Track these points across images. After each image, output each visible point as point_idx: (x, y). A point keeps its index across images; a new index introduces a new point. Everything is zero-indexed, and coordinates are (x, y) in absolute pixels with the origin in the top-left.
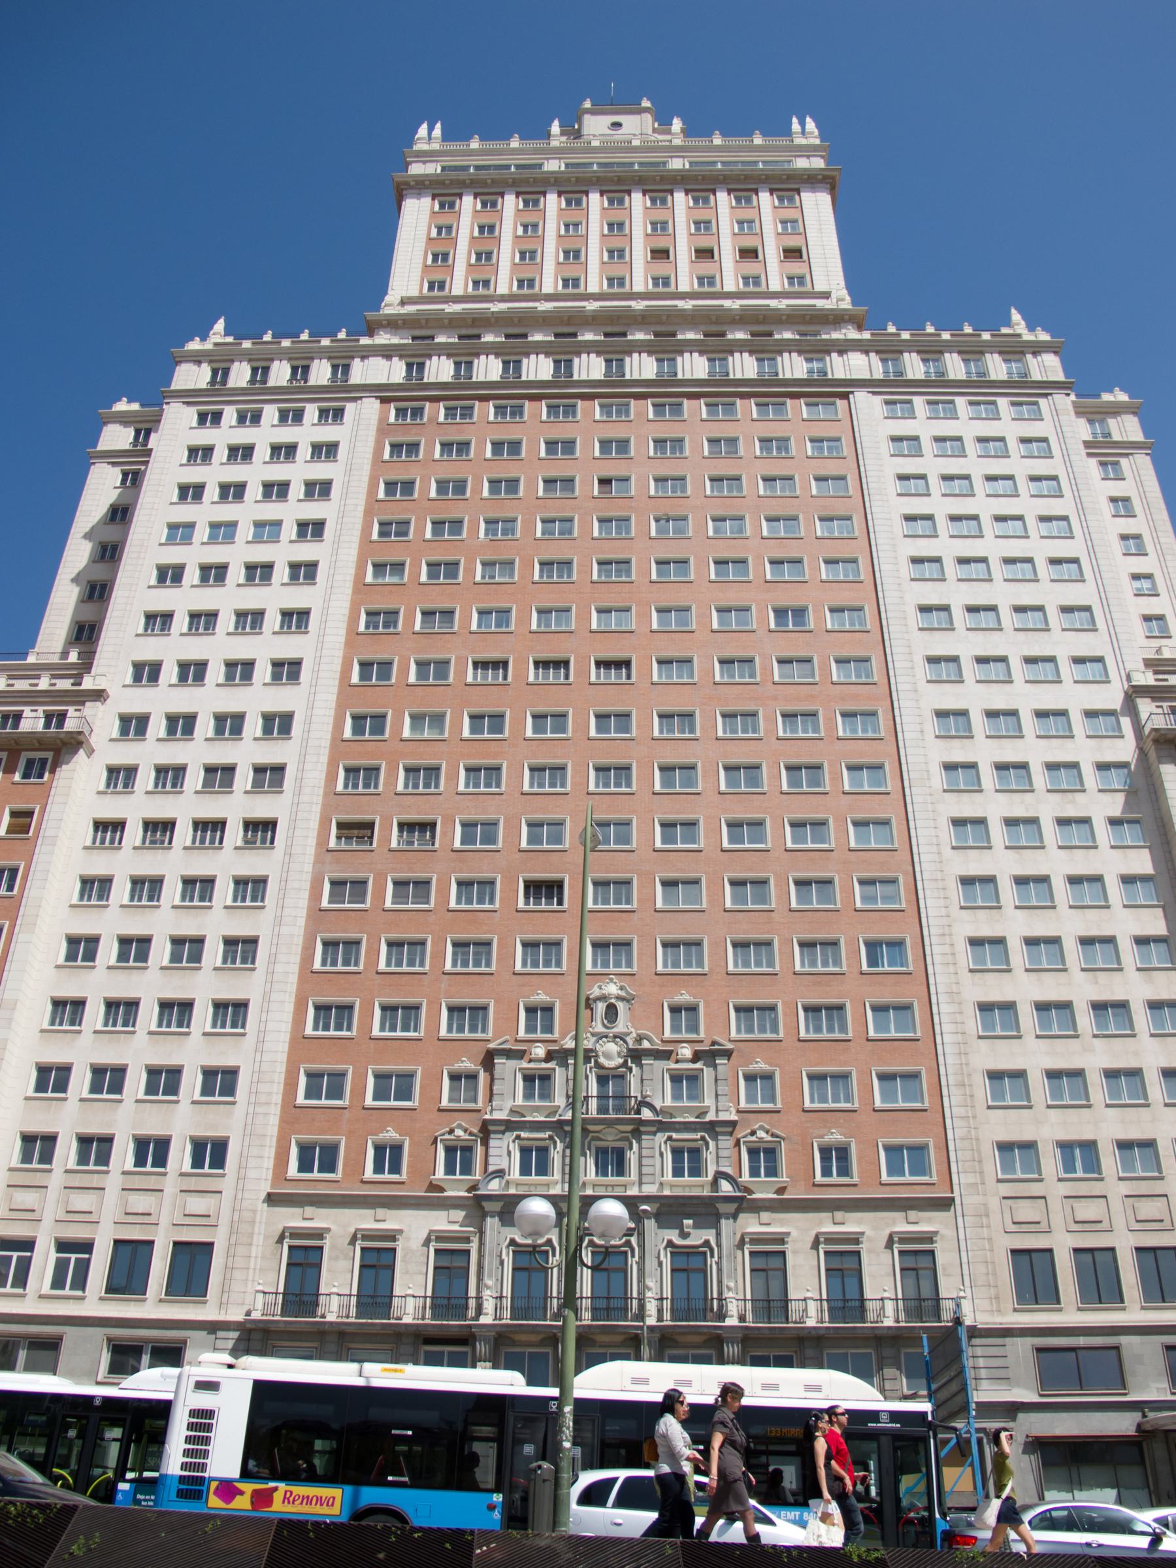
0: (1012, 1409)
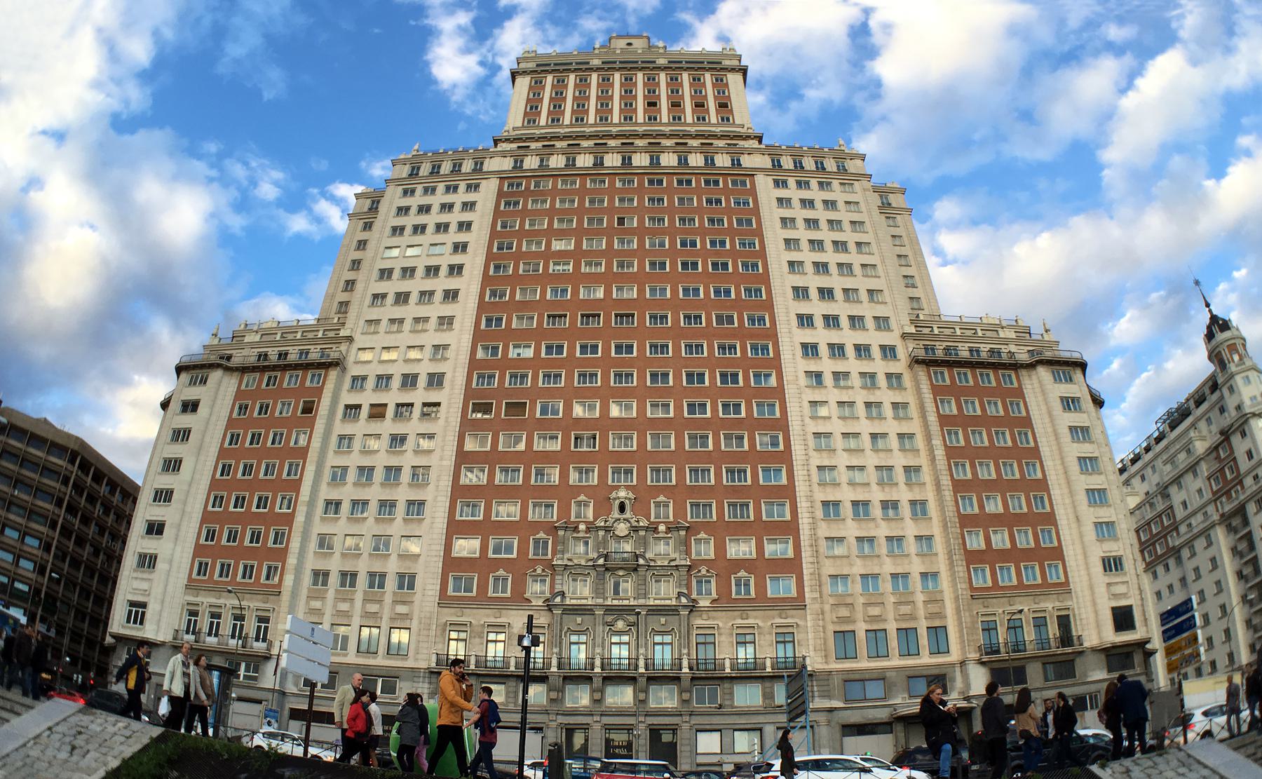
0: (831, 710)
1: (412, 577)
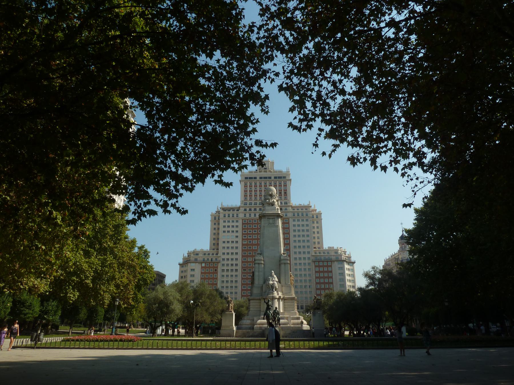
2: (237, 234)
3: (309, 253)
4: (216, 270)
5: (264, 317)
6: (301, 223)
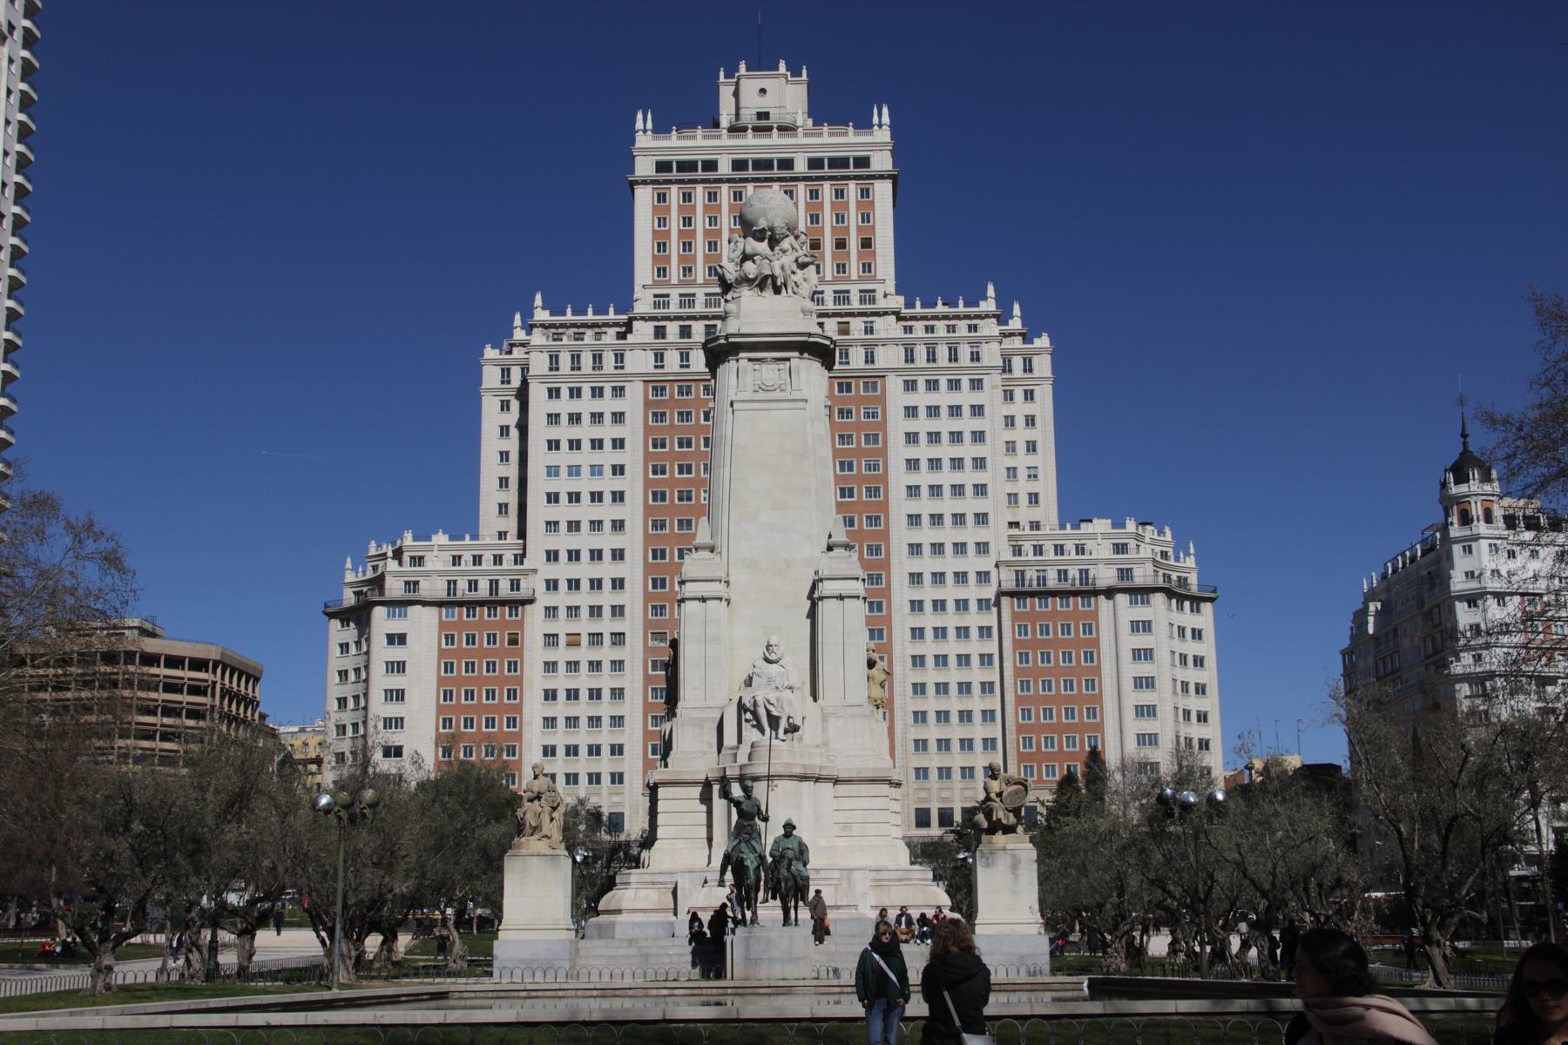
1: (621, 775)
2: (618, 458)
3: (982, 548)
4: (514, 641)
5: (723, 871)
6: (944, 398)
